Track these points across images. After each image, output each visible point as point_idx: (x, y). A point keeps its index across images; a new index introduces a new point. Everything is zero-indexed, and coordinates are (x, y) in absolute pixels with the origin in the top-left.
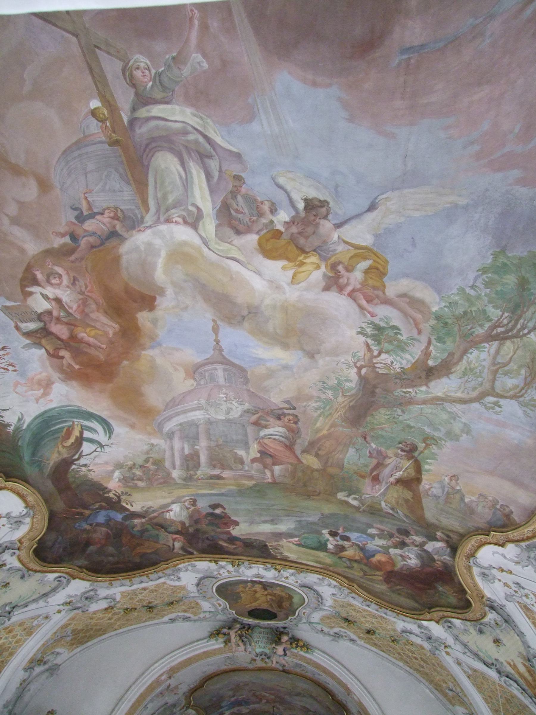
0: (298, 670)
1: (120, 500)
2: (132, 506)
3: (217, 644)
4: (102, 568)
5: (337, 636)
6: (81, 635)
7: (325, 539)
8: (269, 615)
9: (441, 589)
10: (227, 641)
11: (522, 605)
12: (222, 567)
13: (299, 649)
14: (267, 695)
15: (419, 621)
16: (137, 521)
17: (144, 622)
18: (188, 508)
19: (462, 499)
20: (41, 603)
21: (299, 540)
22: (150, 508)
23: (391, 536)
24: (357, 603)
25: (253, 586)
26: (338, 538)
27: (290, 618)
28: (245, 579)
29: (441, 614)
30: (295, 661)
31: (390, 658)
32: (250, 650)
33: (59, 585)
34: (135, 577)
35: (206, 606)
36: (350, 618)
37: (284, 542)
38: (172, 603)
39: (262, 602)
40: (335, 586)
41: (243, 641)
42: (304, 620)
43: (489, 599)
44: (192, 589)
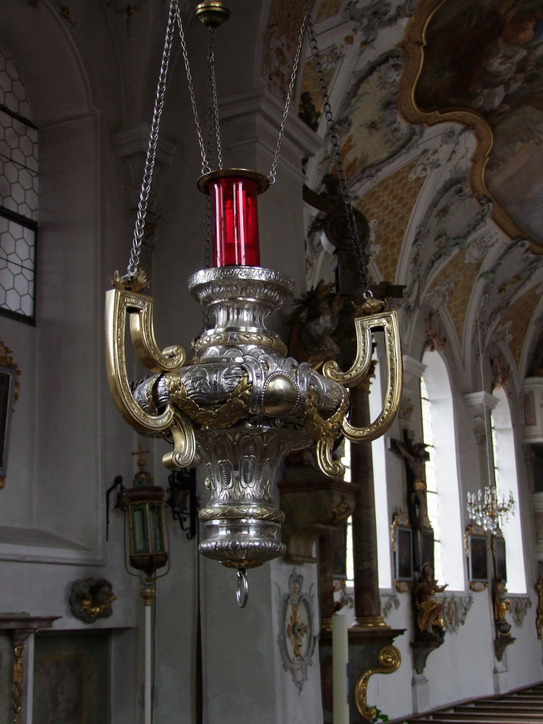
19: (522, 141)
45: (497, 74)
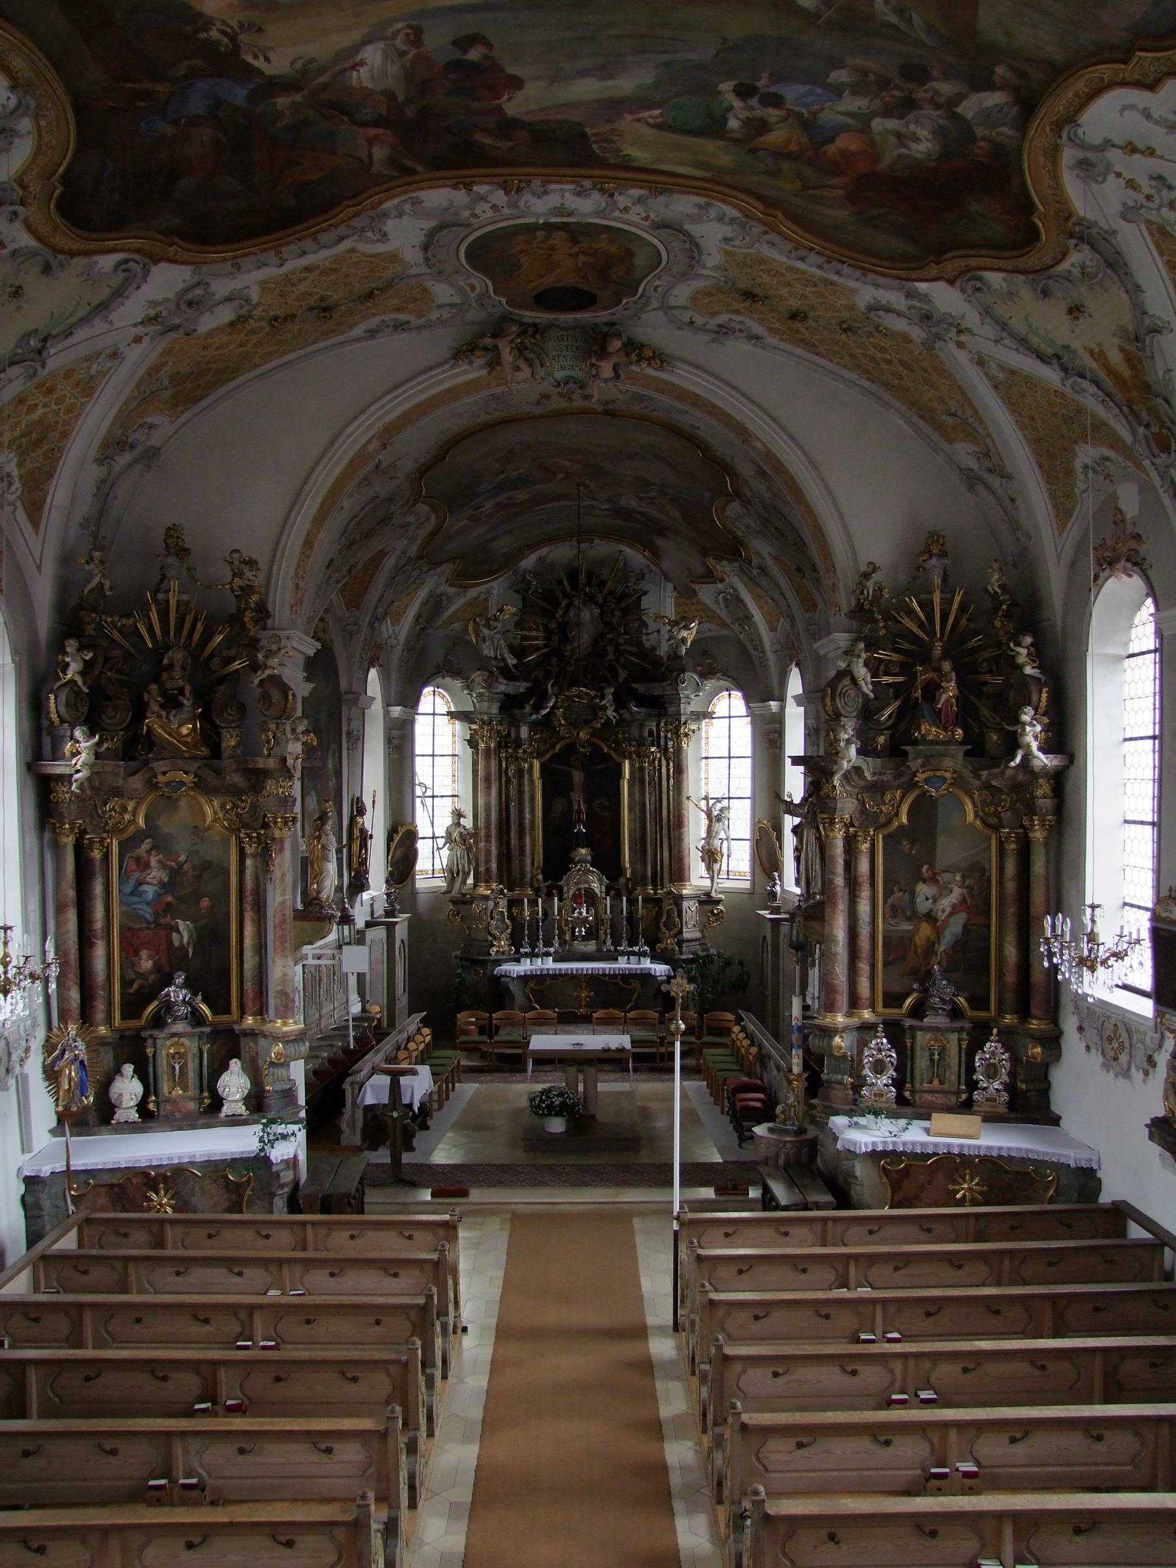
0: (636, 408)
1: (237, 48)
2: (267, 60)
3: (471, 371)
4: (214, 230)
5: (723, 332)
6: (190, 384)
7: (725, 105)
8: (578, 299)
9: (974, 207)
10: (494, 363)
11: (1154, 227)
12: (482, 198)
13: (644, 365)
14: (568, 464)
15: (910, 284)
16: (282, 101)
17: (314, 343)
18: (402, 54)
20: (99, 325)
21: (661, 115)
22: (311, 61)
23: (883, 84)
24: (777, 255)
25: (548, 237)
26: (754, 101)
27: (624, 301)
28: (532, 220)
29: (963, 263)
30: (634, 389)
31: (831, 366)
32: (542, 374)
33: (127, 279)
34: (287, 244)
35: (443, 292)
36: (756, 290)
37: (627, 123)
38: (370, 295)
39: (566, 272)
40: (732, 221)
41: (526, 359)
42: (655, 304)
43: (1081, 222)
44: (412, 256)
45: (940, 133)
